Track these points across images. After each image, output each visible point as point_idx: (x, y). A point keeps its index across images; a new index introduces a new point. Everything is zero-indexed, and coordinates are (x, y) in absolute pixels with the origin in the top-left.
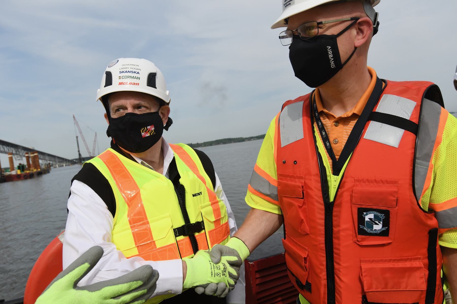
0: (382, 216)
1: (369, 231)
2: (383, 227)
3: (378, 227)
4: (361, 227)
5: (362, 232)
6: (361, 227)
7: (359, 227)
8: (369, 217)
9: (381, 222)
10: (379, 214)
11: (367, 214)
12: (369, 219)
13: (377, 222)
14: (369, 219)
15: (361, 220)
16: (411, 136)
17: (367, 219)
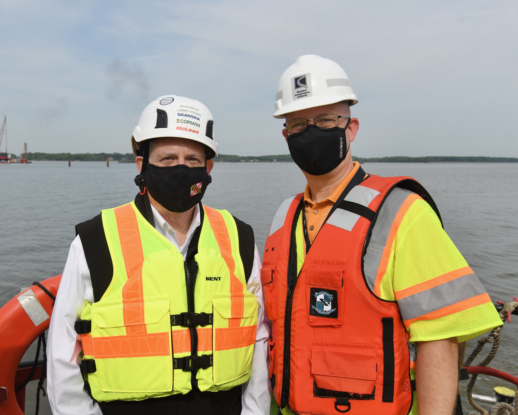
0: (330, 297)
1: (319, 312)
2: (332, 308)
3: (328, 308)
4: (313, 307)
5: (313, 313)
6: (313, 307)
7: (311, 307)
8: (320, 297)
9: (330, 303)
10: (328, 295)
11: (318, 295)
12: (320, 299)
13: (327, 303)
14: (320, 299)
15: (313, 300)
16: (367, 222)
17: (318, 300)
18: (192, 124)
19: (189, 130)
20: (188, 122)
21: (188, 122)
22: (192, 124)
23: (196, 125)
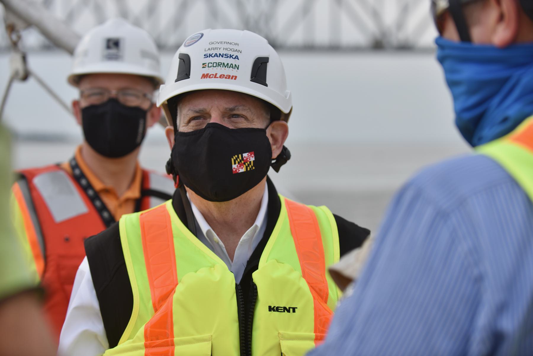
18: (225, 67)
19: (220, 77)
20: (219, 65)
21: (219, 65)
22: (225, 67)
23: (233, 67)
